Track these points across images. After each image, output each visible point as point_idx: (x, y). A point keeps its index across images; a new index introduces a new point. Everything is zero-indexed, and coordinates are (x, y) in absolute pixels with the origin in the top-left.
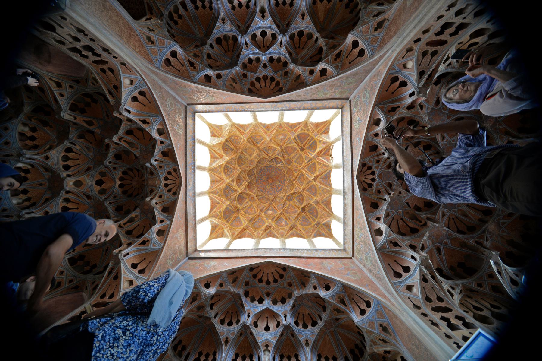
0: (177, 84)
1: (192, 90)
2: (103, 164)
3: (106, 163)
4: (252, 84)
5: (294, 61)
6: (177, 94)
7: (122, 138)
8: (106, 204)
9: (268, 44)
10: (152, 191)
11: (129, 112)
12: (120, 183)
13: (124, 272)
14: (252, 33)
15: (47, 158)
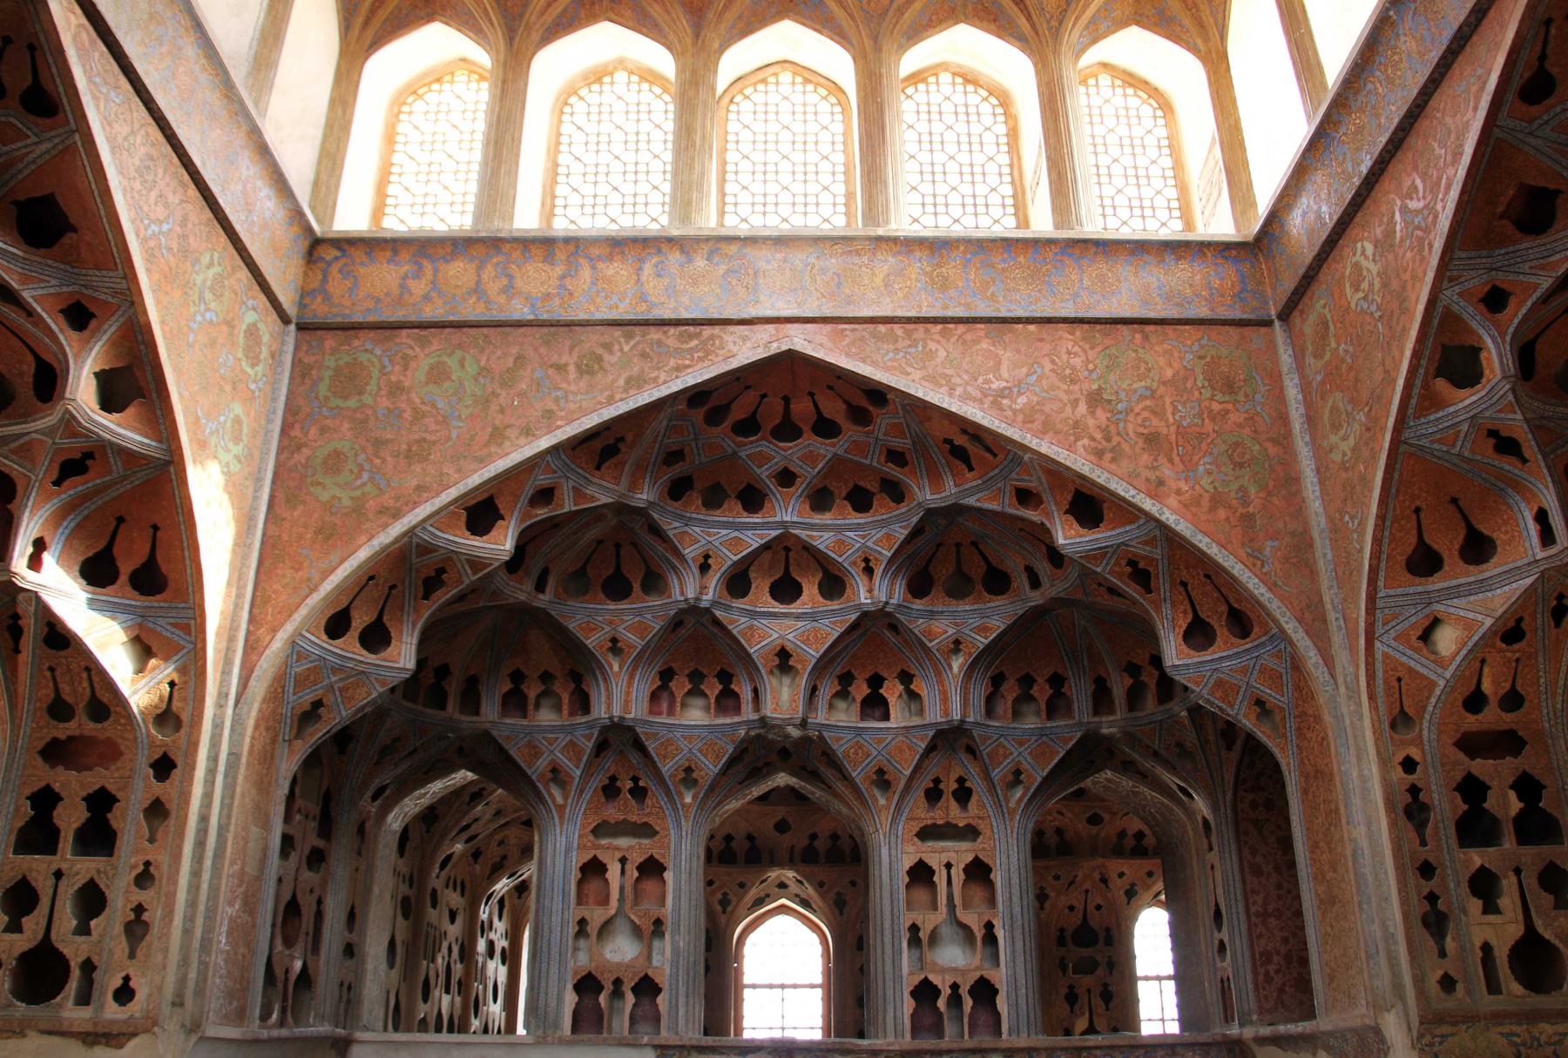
0: (1248, 519)
1: (1189, 465)
4: (860, 416)
6: (1283, 439)
9: (767, 556)
11: (1541, 517)
14: (834, 605)
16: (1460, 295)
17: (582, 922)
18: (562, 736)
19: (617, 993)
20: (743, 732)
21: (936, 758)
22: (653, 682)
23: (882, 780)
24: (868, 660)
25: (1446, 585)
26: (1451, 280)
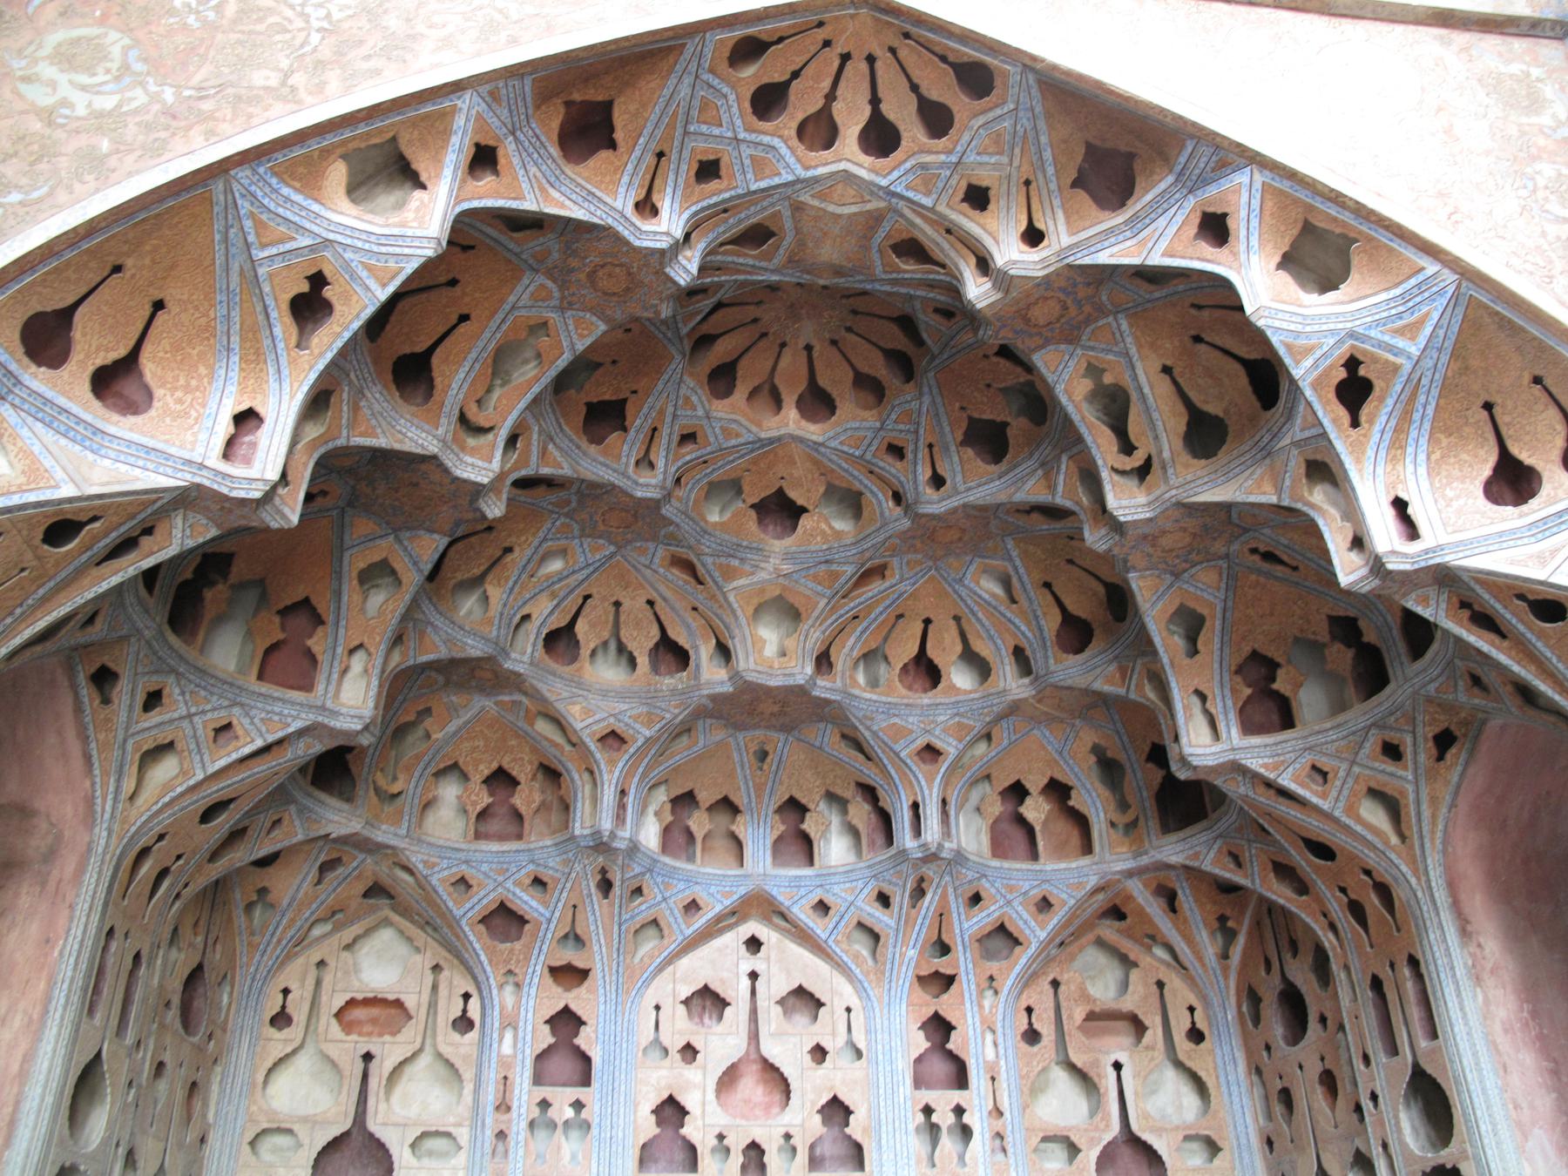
2: (654, 506)
3: (647, 485)
7: (463, 419)
8: (934, 504)
10: (912, 249)
11: (246, 419)
12: (791, 414)
13: (1542, 559)
15: (613, 739)
16: (479, 117)
25: (49, 394)
26: (491, 93)
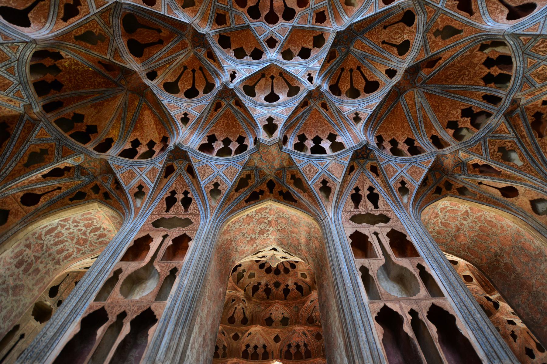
5: (199, 40)
17: (120, 271)
18: (148, 166)
19: (118, 325)
20: (247, 158)
21: (355, 174)
22: (204, 140)
23: (326, 189)
24: (312, 121)
